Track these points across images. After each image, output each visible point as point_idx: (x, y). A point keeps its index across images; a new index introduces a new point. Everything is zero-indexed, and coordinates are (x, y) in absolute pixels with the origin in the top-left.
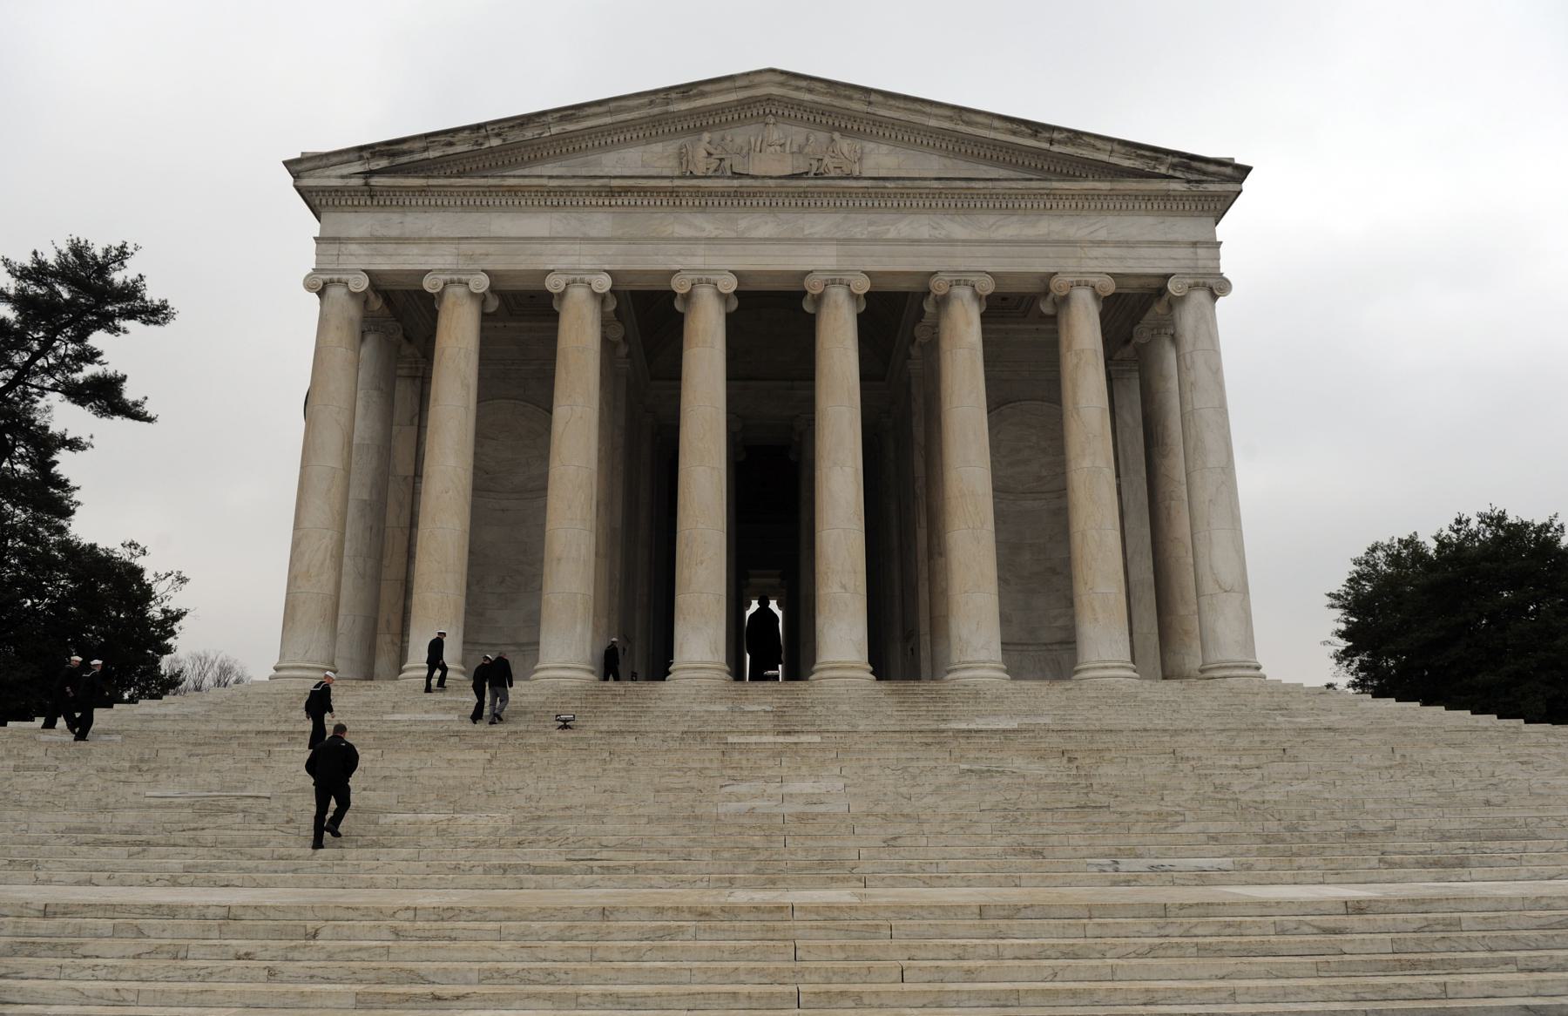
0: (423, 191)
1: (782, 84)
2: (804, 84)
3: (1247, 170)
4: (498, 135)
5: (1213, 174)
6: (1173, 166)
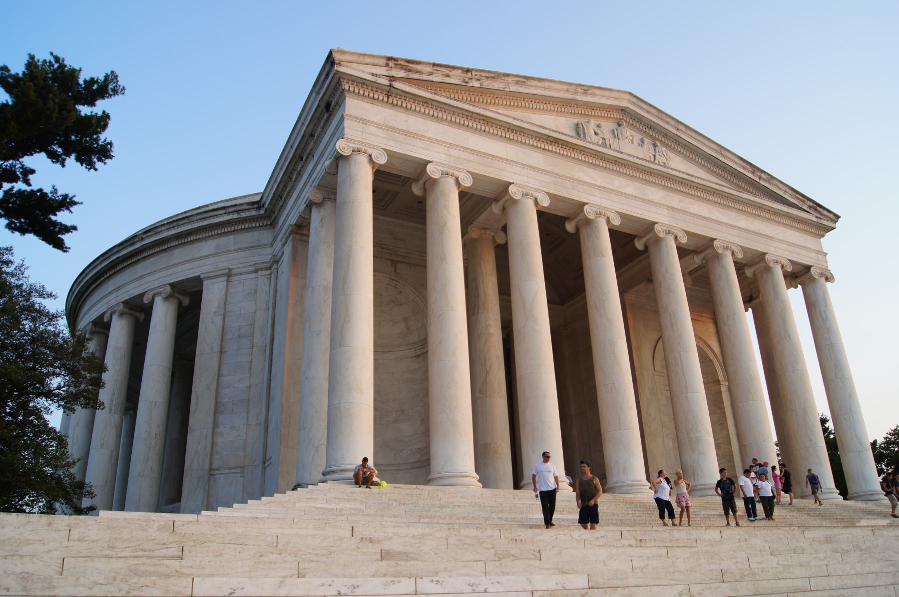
0: (426, 102)
1: (634, 103)
2: (645, 106)
3: (838, 217)
4: (478, 80)
5: (825, 216)
6: (810, 207)
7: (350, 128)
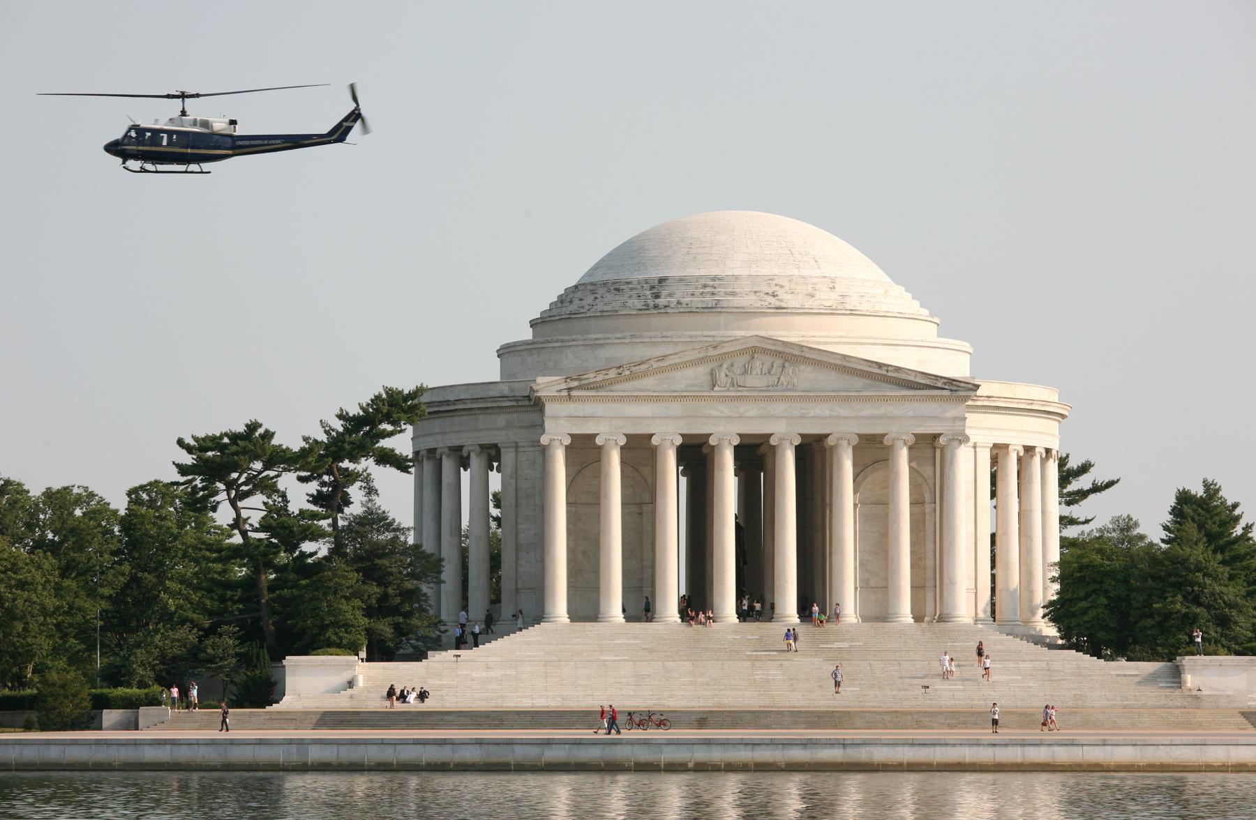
7: (549, 425)
